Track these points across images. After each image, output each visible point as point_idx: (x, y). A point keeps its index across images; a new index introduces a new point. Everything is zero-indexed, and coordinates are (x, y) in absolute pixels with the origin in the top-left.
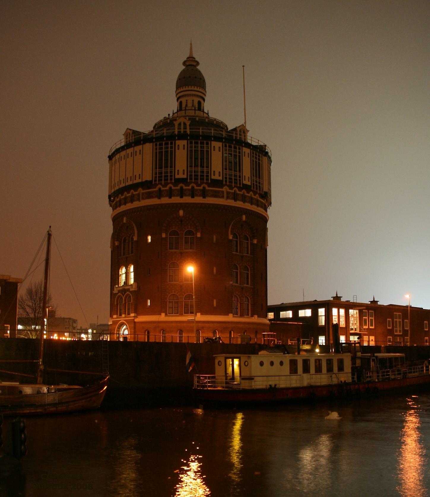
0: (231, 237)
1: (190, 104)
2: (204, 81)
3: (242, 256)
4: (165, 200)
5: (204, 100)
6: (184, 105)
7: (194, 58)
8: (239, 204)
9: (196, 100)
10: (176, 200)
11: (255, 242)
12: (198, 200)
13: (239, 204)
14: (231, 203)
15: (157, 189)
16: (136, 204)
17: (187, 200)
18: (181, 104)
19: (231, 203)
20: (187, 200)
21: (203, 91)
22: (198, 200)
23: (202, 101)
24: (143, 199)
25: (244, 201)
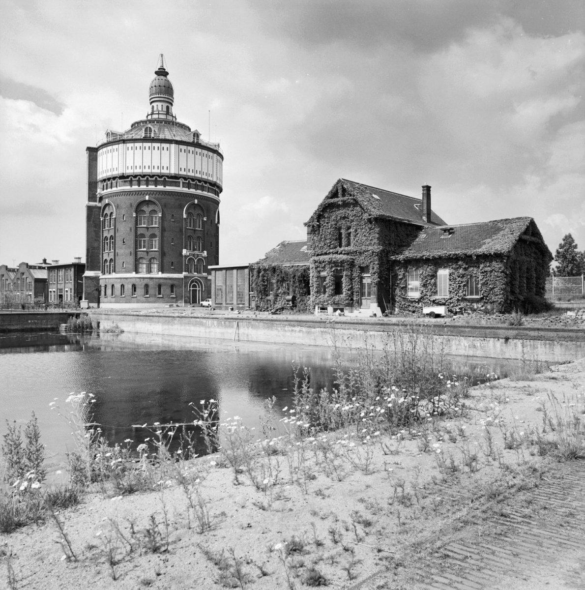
0: (185, 216)
1: (160, 109)
2: (172, 89)
3: (195, 230)
4: (135, 188)
5: (172, 105)
6: (155, 109)
7: (165, 69)
8: (192, 191)
9: (165, 105)
10: (143, 187)
11: (205, 219)
12: (160, 188)
13: (192, 191)
14: (186, 190)
15: (129, 179)
16: (114, 189)
17: (152, 187)
18: (153, 107)
19: (186, 190)
20: (152, 187)
21: (170, 98)
22: (160, 188)
23: (170, 106)
24: (119, 186)
25: (196, 189)
